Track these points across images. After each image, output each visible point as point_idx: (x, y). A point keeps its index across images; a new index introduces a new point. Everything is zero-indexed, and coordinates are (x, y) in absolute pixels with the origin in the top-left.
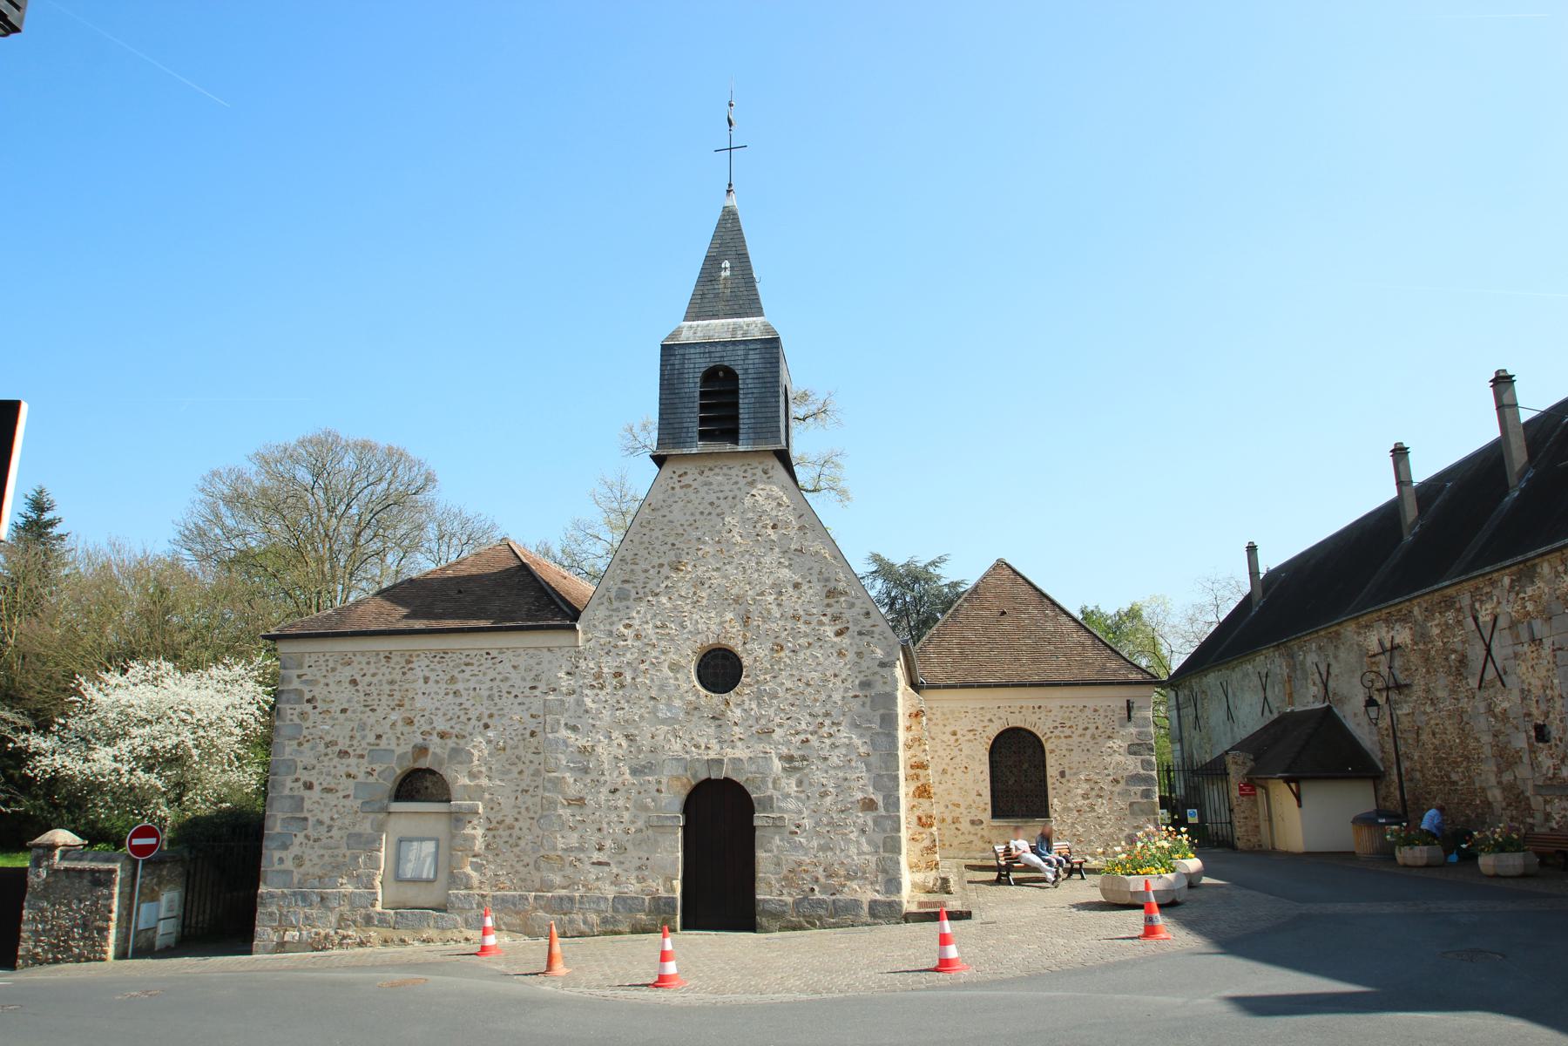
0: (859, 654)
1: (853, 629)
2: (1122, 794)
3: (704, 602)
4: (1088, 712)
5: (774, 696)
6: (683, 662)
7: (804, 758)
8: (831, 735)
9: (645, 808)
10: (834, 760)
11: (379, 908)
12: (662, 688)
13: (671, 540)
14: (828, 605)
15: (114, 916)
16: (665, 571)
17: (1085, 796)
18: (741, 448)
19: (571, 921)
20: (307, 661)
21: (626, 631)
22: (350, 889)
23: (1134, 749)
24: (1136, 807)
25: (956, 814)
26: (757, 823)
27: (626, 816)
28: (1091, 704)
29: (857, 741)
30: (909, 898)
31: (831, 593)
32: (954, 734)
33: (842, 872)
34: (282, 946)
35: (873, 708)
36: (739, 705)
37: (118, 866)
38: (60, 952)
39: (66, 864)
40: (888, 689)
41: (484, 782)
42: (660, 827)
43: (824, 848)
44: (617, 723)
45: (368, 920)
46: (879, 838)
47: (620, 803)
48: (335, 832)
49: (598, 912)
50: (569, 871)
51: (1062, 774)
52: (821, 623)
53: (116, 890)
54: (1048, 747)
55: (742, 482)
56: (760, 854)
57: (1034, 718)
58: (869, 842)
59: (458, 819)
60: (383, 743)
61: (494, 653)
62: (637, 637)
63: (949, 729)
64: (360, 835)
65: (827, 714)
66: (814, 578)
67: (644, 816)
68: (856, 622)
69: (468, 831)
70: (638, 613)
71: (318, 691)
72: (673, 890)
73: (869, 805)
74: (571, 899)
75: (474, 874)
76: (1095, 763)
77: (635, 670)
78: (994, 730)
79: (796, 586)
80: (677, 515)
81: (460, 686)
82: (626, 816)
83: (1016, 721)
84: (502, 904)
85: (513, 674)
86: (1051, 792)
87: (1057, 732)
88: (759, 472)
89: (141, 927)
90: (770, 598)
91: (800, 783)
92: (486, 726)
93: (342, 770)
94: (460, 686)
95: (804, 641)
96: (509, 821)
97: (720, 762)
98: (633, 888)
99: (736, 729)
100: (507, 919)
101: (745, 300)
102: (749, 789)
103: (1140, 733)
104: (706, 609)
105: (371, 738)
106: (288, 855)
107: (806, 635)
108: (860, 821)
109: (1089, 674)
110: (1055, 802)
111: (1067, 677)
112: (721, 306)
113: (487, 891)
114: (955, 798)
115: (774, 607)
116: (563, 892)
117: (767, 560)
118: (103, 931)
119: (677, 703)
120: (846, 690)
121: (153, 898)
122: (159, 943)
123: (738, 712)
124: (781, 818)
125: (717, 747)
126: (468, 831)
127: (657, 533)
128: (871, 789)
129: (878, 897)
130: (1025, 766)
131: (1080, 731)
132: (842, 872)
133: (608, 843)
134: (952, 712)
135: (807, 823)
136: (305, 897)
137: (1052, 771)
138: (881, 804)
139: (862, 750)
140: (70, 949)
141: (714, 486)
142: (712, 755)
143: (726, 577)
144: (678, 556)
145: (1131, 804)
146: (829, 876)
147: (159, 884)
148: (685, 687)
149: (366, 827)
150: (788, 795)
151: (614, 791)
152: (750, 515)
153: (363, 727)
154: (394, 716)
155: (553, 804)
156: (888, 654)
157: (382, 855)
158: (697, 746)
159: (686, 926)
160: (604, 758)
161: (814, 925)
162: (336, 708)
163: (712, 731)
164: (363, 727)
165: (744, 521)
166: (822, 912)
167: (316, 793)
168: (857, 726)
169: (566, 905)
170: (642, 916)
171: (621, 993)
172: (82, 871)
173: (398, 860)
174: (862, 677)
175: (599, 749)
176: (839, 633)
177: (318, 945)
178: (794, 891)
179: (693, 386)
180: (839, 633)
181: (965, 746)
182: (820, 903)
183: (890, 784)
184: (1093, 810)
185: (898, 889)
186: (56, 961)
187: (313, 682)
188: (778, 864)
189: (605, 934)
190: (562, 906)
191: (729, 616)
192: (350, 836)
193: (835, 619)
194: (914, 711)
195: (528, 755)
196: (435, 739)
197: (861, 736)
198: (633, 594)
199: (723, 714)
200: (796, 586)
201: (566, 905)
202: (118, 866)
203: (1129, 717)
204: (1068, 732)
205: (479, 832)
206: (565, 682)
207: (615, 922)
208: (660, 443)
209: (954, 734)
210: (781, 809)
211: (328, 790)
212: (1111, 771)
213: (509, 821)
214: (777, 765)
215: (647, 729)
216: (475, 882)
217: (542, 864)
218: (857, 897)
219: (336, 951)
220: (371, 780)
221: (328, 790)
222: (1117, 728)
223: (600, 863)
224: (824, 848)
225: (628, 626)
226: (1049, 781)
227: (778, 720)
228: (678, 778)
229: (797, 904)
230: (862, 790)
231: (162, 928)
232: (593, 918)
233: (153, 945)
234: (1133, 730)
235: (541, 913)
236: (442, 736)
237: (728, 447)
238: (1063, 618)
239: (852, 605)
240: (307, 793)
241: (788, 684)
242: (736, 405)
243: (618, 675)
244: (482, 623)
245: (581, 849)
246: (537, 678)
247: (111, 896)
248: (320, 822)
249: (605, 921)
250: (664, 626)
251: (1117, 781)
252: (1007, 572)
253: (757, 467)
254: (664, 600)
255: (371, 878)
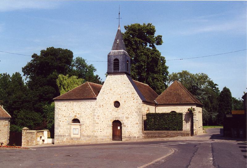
35: (138, 110)
47: (104, 123)
48: (64, 127)
65: (132, 111)
71: (60, 108)
80: (111, 82)
93: (65, 119)
94: (81, 107)
97: (117, 117)
133: (102, 129)
151: (103, 122)
179: (112, 61)
211: (63, 122)
213: (88, 126)
220: (69, 120)
221: (63, 122)
240: (60, 122)
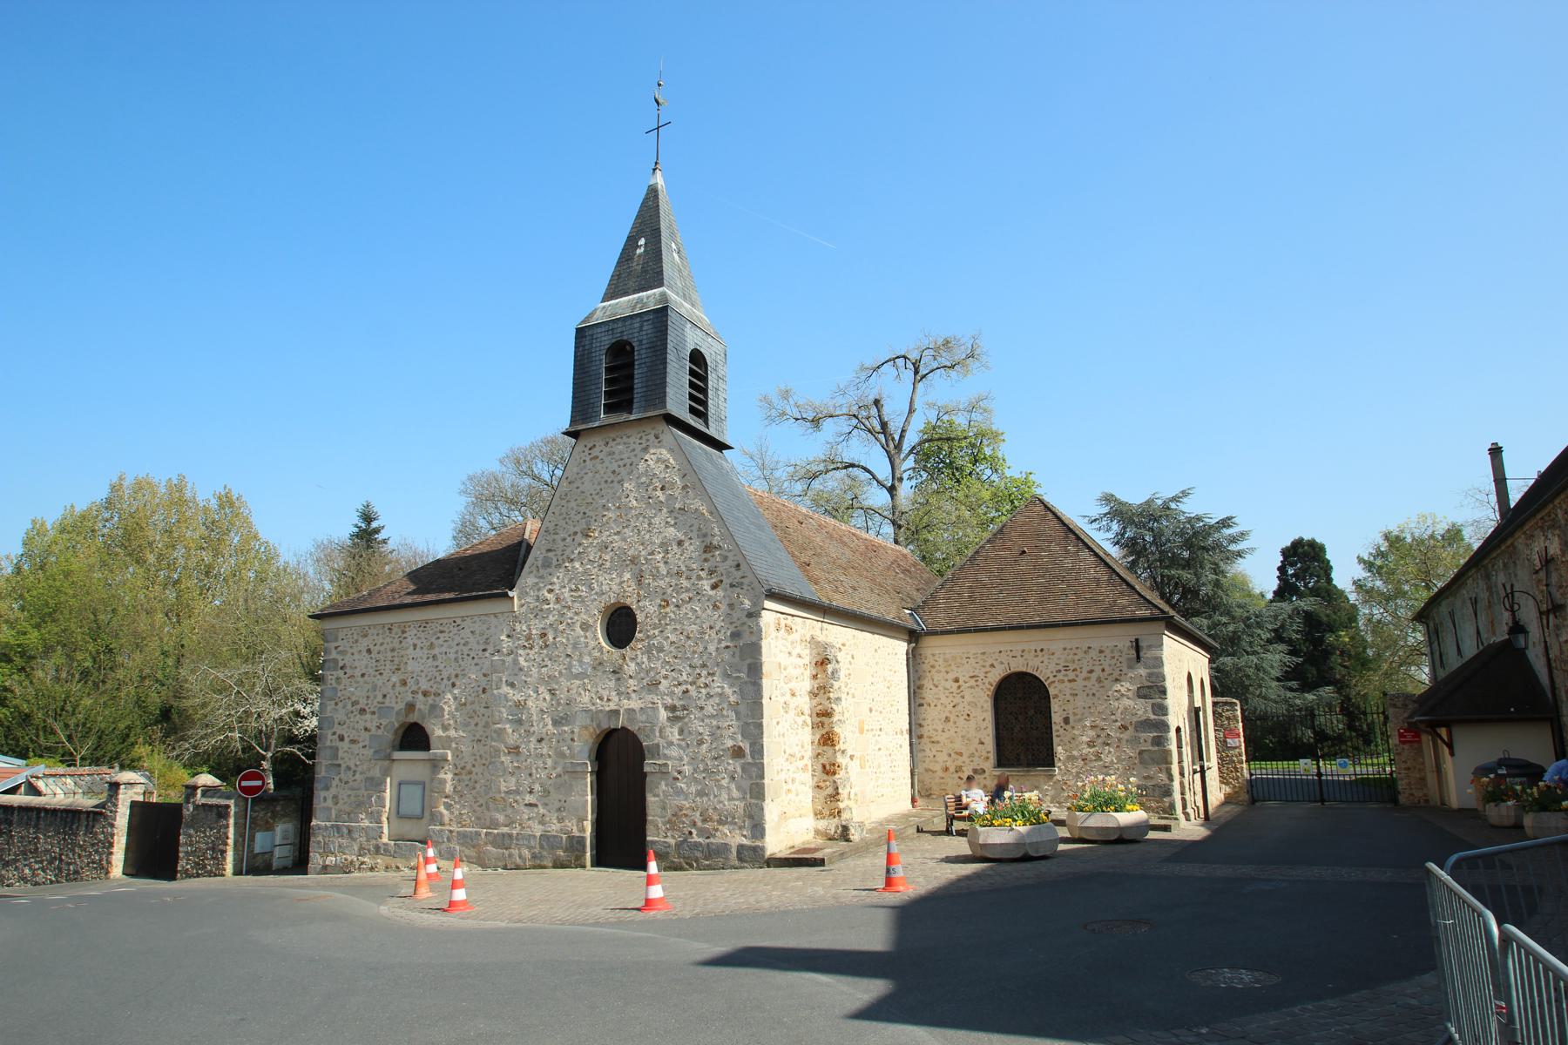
0: (731, 606)
1: (727, 581)
2: (1134, 741)
3: (608, 565)
4: (1093, 653)
5: (661, 650)
6: (591, 621)
7: (684, 708)
8: (706, 685)
9: (562, 755)
10: (709, 710)
11: (385, 839)
12: (575, 646)
13: (583, 509)
14: (706, 560)
15: (231, 841)
16: (579, 537)
17: (1091, 744)
18: (632, 417)
19: (510, 856)
20: (341, 635)
21: (549, 596)
22: (366, 823)
23: (1144, 692)
24: (1146, 756)
25: (959, 763)
26: (646, 769)
27: (549, 762)
28: (1096, 645)
29: (728, 691)
30: (776, 843)
31: (708, 548)
32: (957, 680)
33: (716, 817)
34: (325, 869)
35: (742, 659)
36: (634, 659)
37: (231, 803)
38: (201, 870)
39: (204, 801)
40: (754, 639)
41: (452, 733)
42: (574, 773)
43: (701, 793)
44: (541, 680)
45: (377, 848)
46: (746, 784)
47: (545, 751)
48: (357, 776)
49: (530, 848)
50: (510, 811)
51: (1066, 720)
52: (699, 578)
53: (232, 821)
54: (1052, 691)
55: (639, 448)
56: (650, 798)
57: (1037, 662)
58: (738, 788)
59: (436, 764)
60: (387, 700)
61: (459, 621)
62: (558, 600)
63: (951, 676)
64: (372, 779)
65: (704, 666)
66: (694, 535)
67: (562, 761)
68: (728, 574)
69: (442, 776)
70: (558, 578)
71: (348, 660)
72: (583, 830)
73: (738, 753)
74: (510, 836)
75: (445, 812)
76: (1100, 708)
77: (556, 630)
78: (996, 676)
79: (680, 543)
80: (588, 487)
81: (436, 651)
82: (549, 762)
83: (1018, 666)
84: (464, 838)
85: (472, 640)
86: (1056, 740)
87: (1060, 676)
88: (652, 437)
89: (257, 850)
90: (659, 557)
91: (681, 732)
92: (454, 685)
93: (362, 725)
94: (436, 651)
95: (685, 596)
96: (469, 767)
97: (616, 713)
98: (554, 827)
99: (631, 681)
100: (467, 852)
101: (652, 274)
102: (641, 737)
103: (1150, 675)
104: (609, 571)
105: (380, 698)
106: (329, 794)
107: (688, 590)
108: (731, 768)
109: (1094, 613)
110: (1059, 751)
111: (1070, 617)
112: (631, 283)
113: (454, 828)
114: (958, 746)
115: (661, 565)
116: (505, 830)
117: (656, 521)
118: (223, 852)
119: (587, 659)
120: (720, 641)
121: (269, 828)
122: (275, 864)
123: (633, 665)
124: (666, 765)
125: (616, 699)
126: (442, 776)
127: (573, 504)
128: (739, 737)
129: (745, 841)
130: (1031, 712)
131: (1085, 674)
132: (716, 817)
133: (537, 787)
134: (954, 658)
135: (687, 769)
136: (338, 828)
137: (1056, 718)
138: (748, 751)
139: (732, 699)
140: (204, 867)
141: (617, 456)
142: (612, 706)
143: (624, 540)
144: (588, 523)
145: (1141, 753)
146: (705, 821)
147: (273, 817)
148: (592, 644)
149: (376, 772)
150: (671, 744)
151: (540, 741)
152: (643, 479)
153: (375, 688)
154: (394, 679)
155: (498, 751)
156: (754, 604)
157: (388, 795)
158: (601, 699)
159: (599, 862)
160: (533, 711)
161: (691, 866)
162: (358, 673)
163: (612, 684)
164: (375, 688)
165: (639, 485)
166: (698, 854)
167: (345, 745)
168: (729, 676)
169: (507, 842)
170: (561, 853)
171: (425, 916)
172: (211, 806)
173: (398, 800)
174: (732, 629)
175: (530, 703)
176: (714, 587)
177: (345, 869)
178: (676, 834)
179: (602, 364)
180: (714, 587)
181: (967, 693)
182: (697, 845)
183: (756, 732)
184: (1099, 759)
185: (762, 835)
186: (198, 876)
187: (343, 653)
188: (664, 808)
189: (534, 867)
190: (503, 841)
191: (627, 576)
192: (367, 779)
193: (711, 573)
194: (819, 659)
195: (479, 710)
196: (420, 696)
197: (731, 686)
198: (555, 562)
199: (621, 667)
200: (680, 543)
201: (507, 842)
202: (231, 803)
203: (1138, 658)
204: (1071, 675)
205: (449, 776)
206: (507, 645)
207: (541, 857)
208: (573, 422)
209: (957, 680)
210: (666, 757)
211: (353, 742)
212: (1118, 716)
213: (469, 767)
214: (663, 714)
215: (564, 683)
216: (446, 820)
217: (492, 806)
218: (727, 841)
219: (357, 874)
220: (380, 732)
221: (353, 742)
222: (1125, 669)
223: (530, 805)
224: (701, 793)
225: (550, 591)
226: (1054, 727)
227: (664, 672)
228: (586, 728)
229: (679, 845)
230: (732, 738)
231: (277, 852)
232: (526, 853)
233: (270, 865)
234: (1143, 672)
235: (489, 848)
236: (425, 694)
237: (624, 417)
238: (1085, 554)
239: (725, 558)
240: (340, 744)
241: (673, 637)
242: (632, 377)
243: (543, 635)
244: (447, 596)
245: (517, 792)
246: (487, 642)
247: (227, 826)
248: (349, 768)
249: (534, 857)
250: (577, 590)
251: (1125, 728)
252: (1040, 508)
253: (650, 431)
254: (577, 565)
255: (380, 814)
